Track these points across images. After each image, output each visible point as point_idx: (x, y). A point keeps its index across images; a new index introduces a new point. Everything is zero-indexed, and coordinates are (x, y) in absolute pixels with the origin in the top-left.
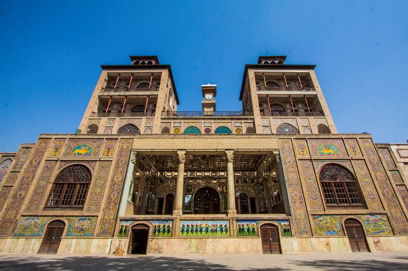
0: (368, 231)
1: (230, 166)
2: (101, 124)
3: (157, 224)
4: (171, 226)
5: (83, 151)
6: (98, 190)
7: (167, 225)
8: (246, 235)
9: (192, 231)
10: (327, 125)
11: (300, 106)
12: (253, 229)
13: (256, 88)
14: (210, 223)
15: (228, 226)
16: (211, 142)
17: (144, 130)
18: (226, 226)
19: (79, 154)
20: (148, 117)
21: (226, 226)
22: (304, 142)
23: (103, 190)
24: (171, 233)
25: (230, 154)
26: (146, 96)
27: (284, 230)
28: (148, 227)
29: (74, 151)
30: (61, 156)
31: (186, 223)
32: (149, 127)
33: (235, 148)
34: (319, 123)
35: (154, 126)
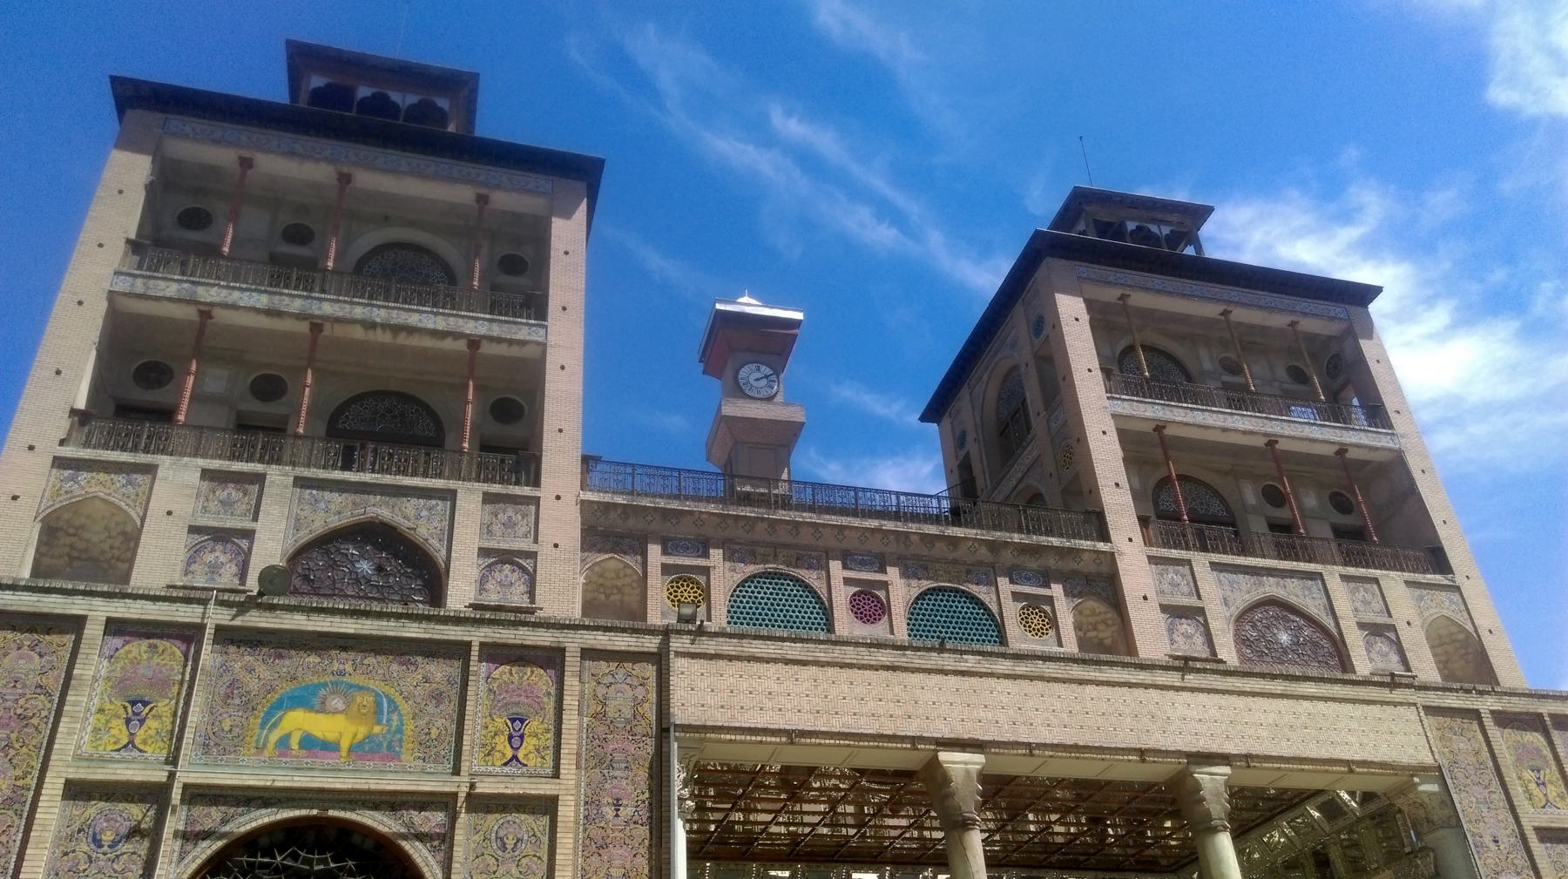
2: (157, 506)
5: (324, 726)
10: (1469, 627)
11: (1311, 501)
13: (1098, 375)
16: (1104, 707)
17: (475, 573)
19: (310, 743)
20: (496, 488)
22: (1535, 739)
25: (1212, 781)
26: (461, 345)
29: (269, 722)
32: (506, 557)
34: (1434, 612)
35: (544, 551)
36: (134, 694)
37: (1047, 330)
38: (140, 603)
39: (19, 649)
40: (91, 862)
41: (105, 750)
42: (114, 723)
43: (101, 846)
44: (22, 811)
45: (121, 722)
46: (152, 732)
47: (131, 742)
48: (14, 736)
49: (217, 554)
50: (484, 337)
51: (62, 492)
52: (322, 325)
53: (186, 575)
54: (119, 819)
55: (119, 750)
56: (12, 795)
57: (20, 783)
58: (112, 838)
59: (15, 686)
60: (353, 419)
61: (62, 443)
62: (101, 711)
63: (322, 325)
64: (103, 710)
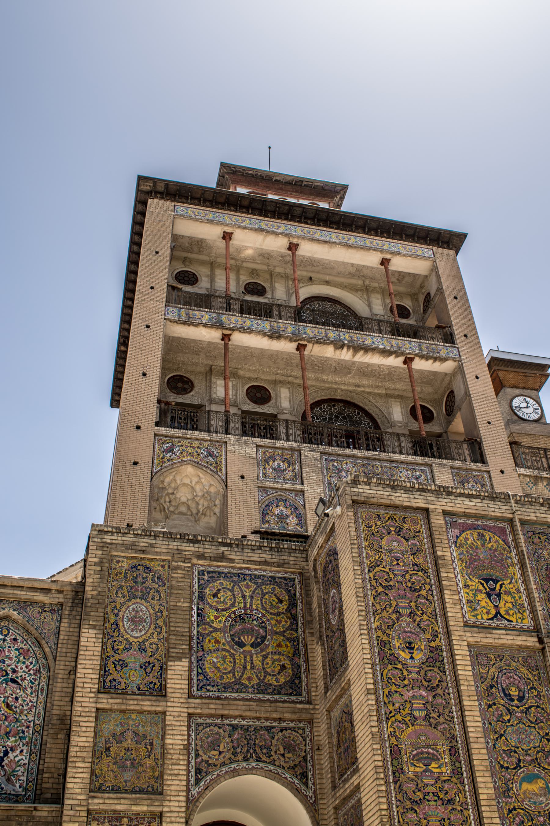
36: (485, 573)
38: (460, 500)
39: (389, 533)
40: (510, 713)
41: (482, 618)
42: (480, 596)
43: (513, 700)
44: (444, 668)
45: (484, 596)
46: (510, 605)
47: (498, 613)
48: (413, 604)
49: (281, 508)
50: (416, 355)
51: (165, 460)
52: (306, 346)
53: (264, 523)
54: (516, 677)
55: (492, 619)
56: (432, 655)
57: (433, 644)
58: (517, 693)
59: (398, 564)
60: (317, 419)
61: (157, 424)
62: (466, 586)
63: (306, 346)
64: (468, 586)
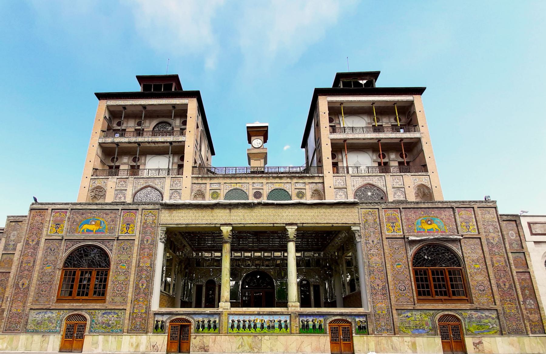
0: (468, 330)
1: (291, 246)
3: (200, 319)
4: (217, 322)
6: (122, 278)
7: (212, 320)
8: (311, 333)
9: (244, 327)
12: (320, 326)
13: (328, 128)
14: (266, 318)
15: (288, 322)
18: (286, 321)
21: (286, 321)
23: (127, 279)
24: (217, 329)
27: (359, 327)
28: (189, 322)
30: (63, 233)
31: (236, 318)
33: (298, 222)
37: (318, 117)
